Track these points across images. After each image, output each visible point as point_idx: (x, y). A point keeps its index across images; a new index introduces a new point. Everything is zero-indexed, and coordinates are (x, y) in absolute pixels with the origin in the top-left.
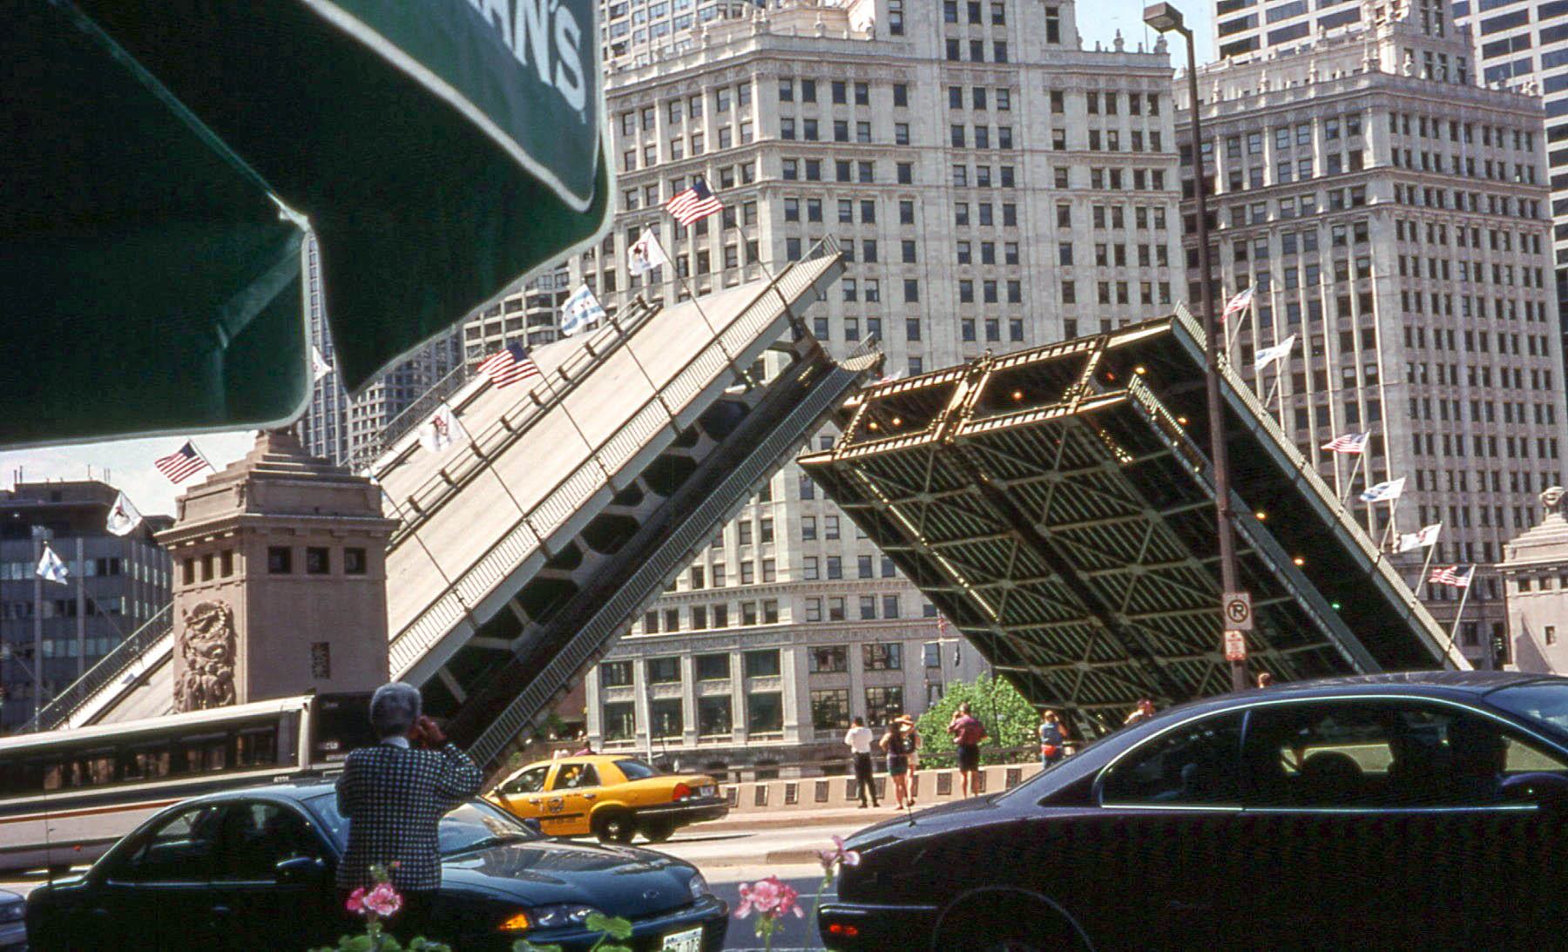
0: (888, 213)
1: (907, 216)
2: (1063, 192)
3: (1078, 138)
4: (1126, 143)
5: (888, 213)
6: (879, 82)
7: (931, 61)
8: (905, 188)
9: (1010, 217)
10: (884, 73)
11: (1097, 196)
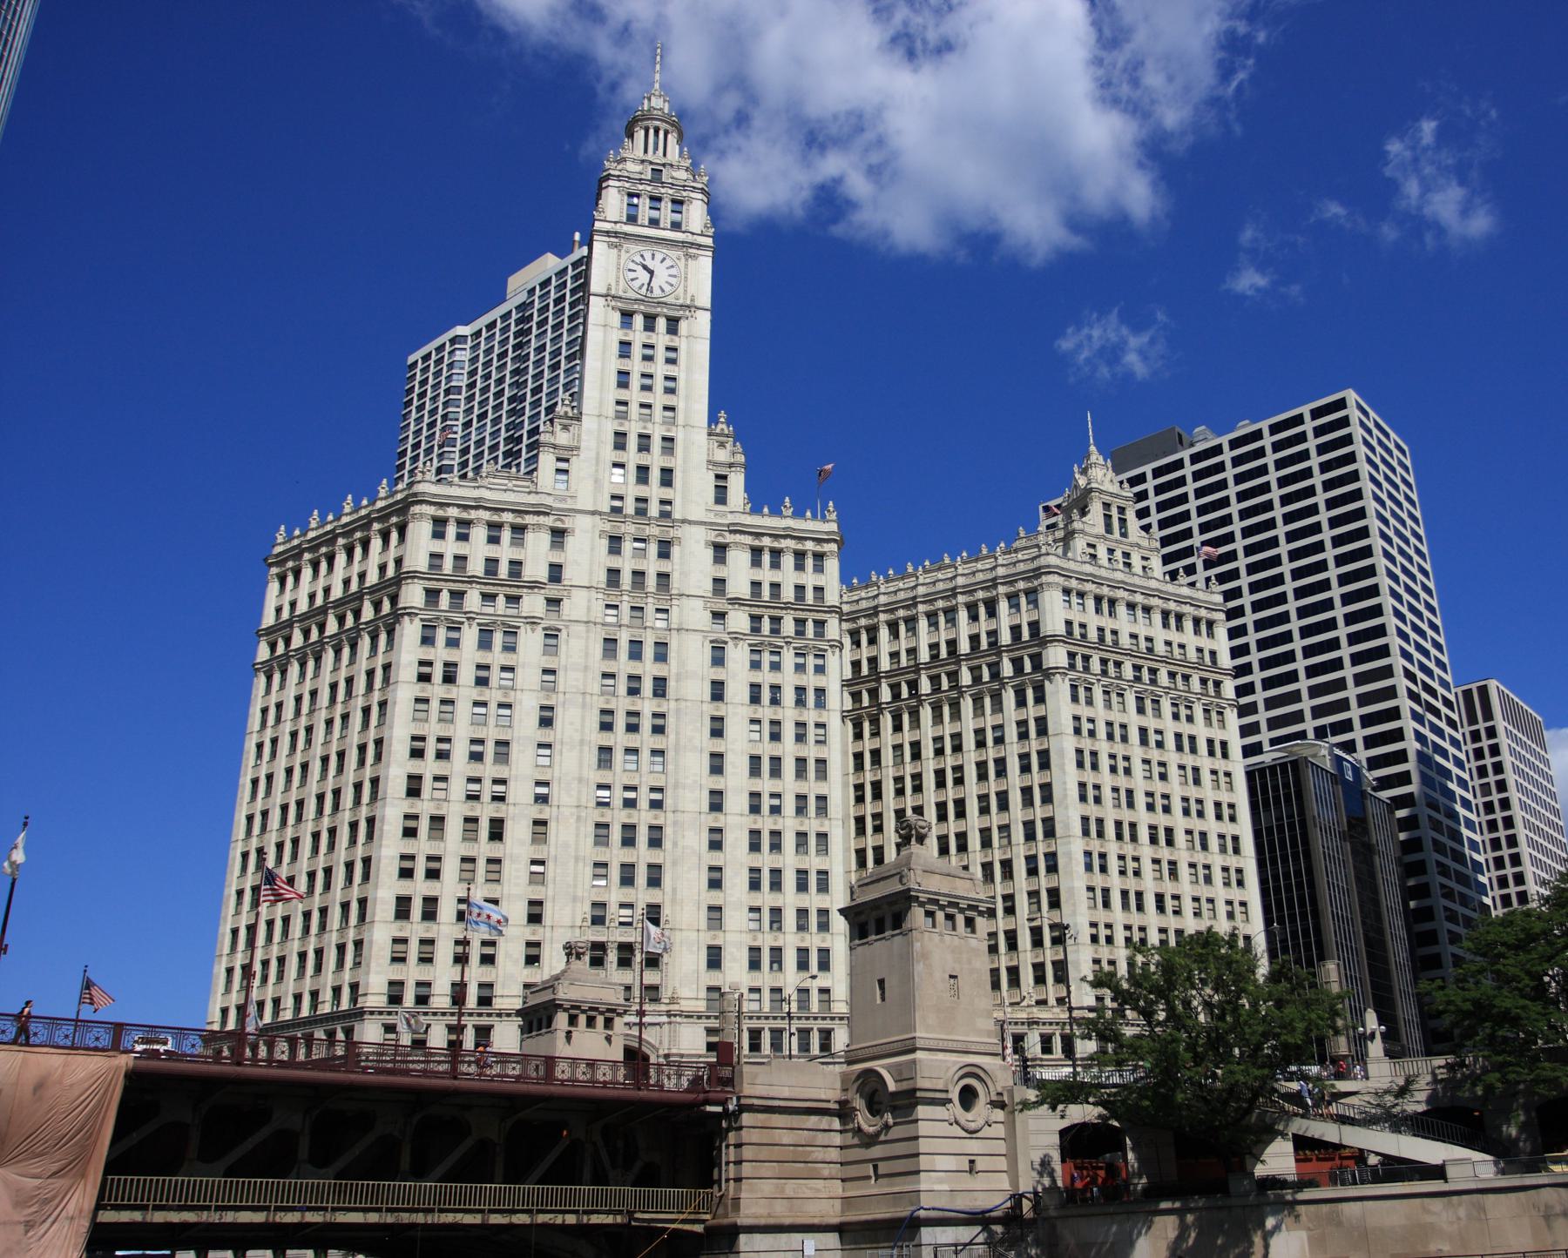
3: (739, 586)
4: (788, 594)
5: (530, 642)
7: (593, 513)
11: (756, 639)
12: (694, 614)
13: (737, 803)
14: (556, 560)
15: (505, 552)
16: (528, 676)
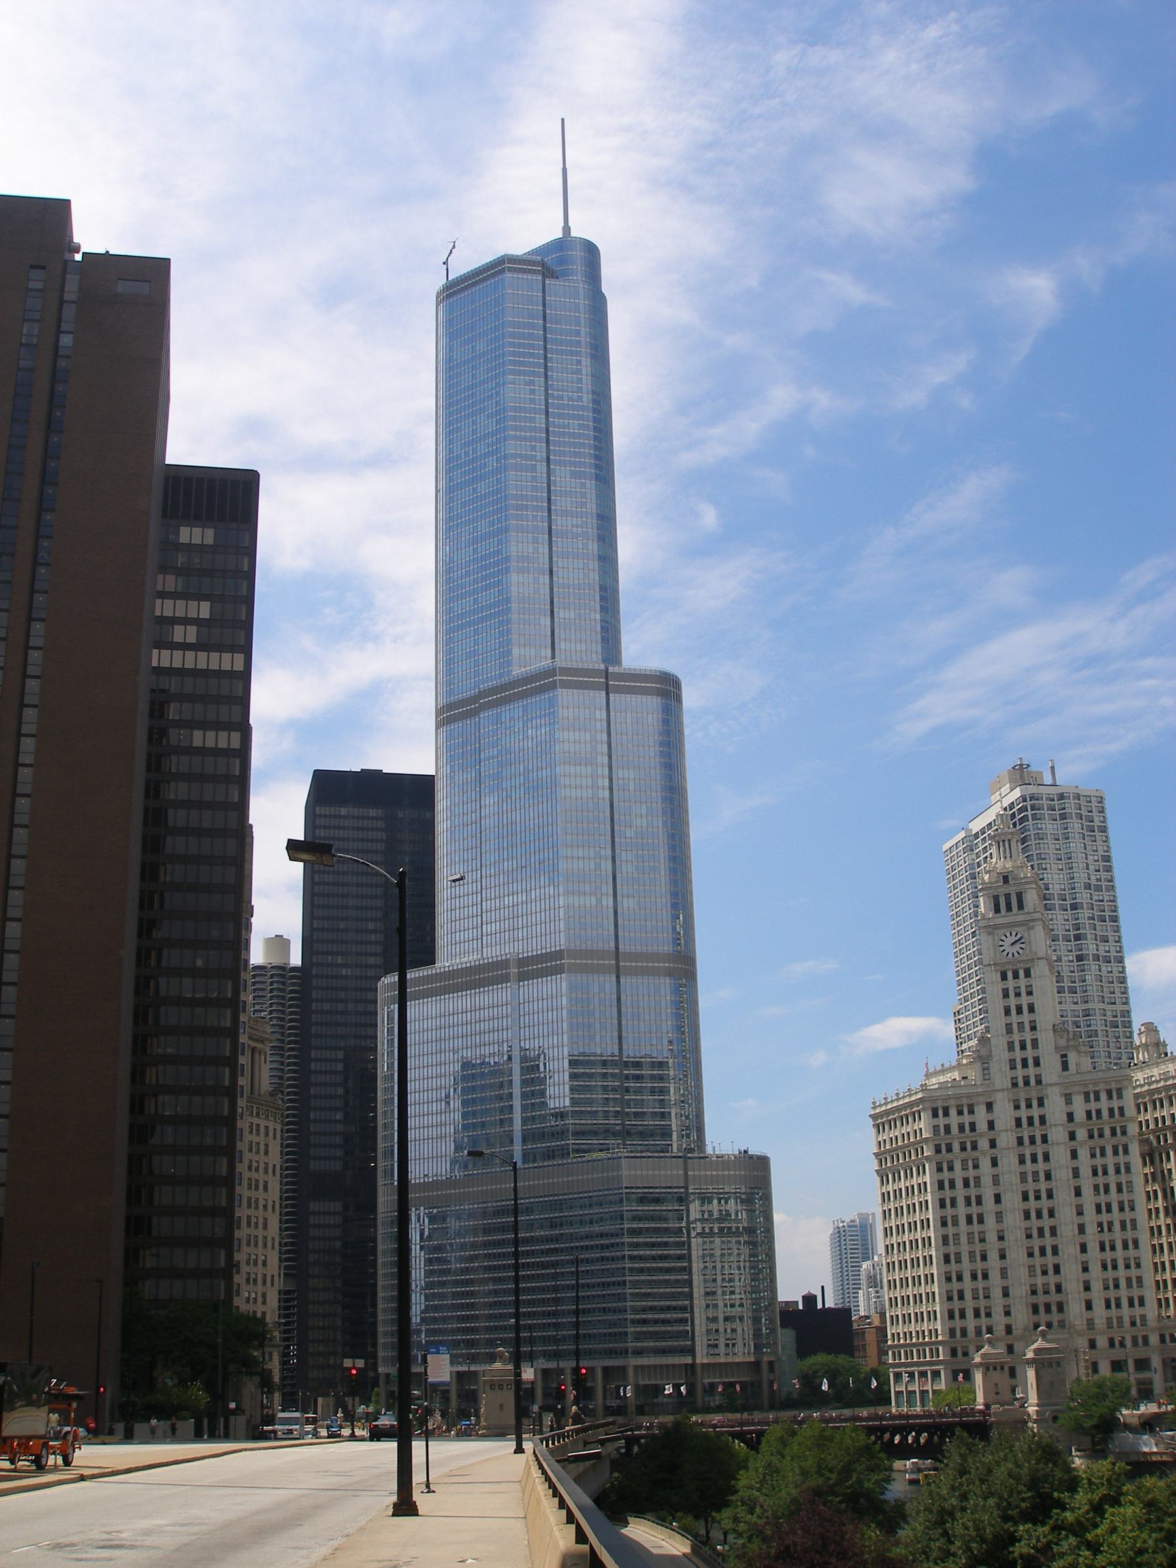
0: (985, 1163)
1: (994, 1163)
2: (1073, 1143)
3: (1080, 1115)
6: (978, 1104)
8: (994, 1151)
9: (1046, 1157)
10: (981, 1099)
11: (1092, 1143)
12: (1058, 1134)
13: (1091, 1229)
14: (990, 1119)
16: (987, 1181)
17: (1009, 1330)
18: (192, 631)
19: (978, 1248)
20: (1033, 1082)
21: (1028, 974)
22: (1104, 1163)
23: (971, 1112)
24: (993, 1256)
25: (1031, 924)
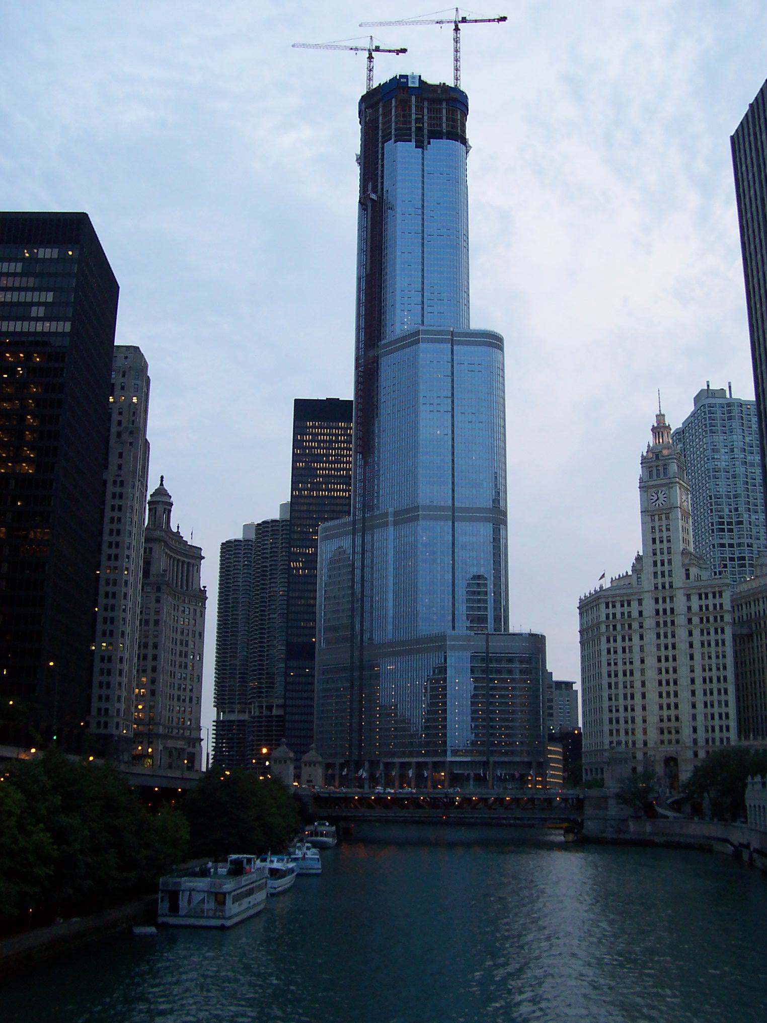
0: (636, 638)
1: (642, 638)
2: (690, 626)
4: (711, 608)
5: (636, 638)
6: (634, 600)
11: (702, 626)
12: (681, 620)
14: (640, 610)
15: (626, 609)
16: (636, 649)
17: (645, 743)
18: (42, 309)
19: (629, 691)
20: (667, 586)
21: (667, 518)
22: (709, 639)
23: (629, 605)
24: (638, 696)
25: (671, 485)
